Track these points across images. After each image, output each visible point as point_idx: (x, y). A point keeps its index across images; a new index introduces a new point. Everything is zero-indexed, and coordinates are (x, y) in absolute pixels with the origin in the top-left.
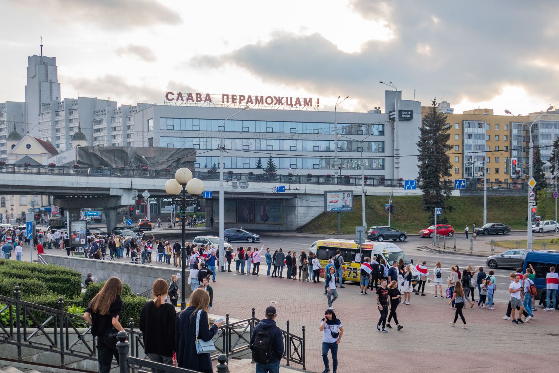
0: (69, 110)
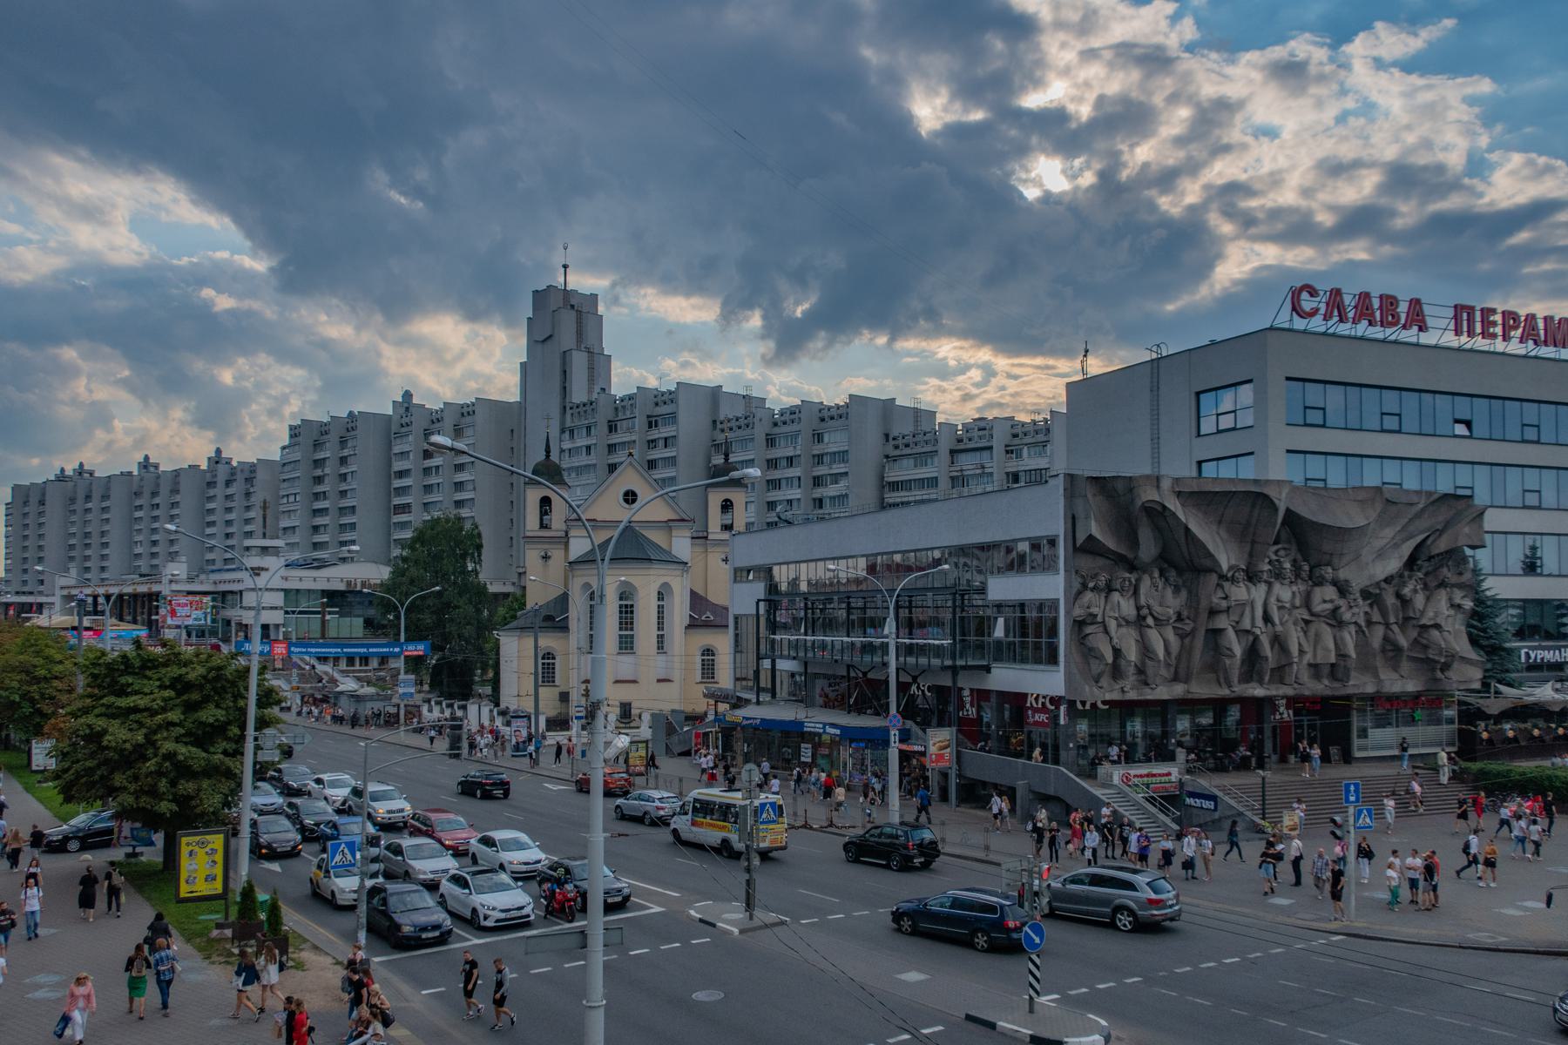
0: (648, 417)
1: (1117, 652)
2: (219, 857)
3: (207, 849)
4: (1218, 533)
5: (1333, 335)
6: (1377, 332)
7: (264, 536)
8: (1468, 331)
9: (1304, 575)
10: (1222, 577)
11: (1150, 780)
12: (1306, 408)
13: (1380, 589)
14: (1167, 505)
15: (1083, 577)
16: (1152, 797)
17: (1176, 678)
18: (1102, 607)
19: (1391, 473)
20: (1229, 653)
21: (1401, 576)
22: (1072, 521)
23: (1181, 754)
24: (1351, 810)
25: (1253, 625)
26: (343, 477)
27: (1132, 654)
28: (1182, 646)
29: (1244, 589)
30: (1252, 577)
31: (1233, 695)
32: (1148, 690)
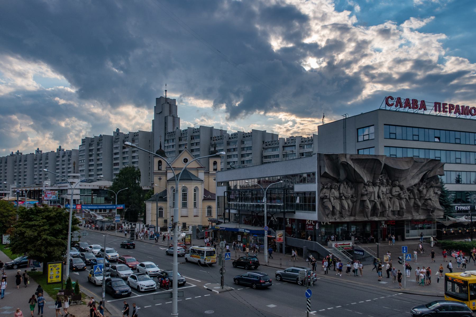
0: (191, 136)
1: (333, 207)
2: (60, 270)
3: (56, 268)
4: (364, 171)
5: (398, 111)
6: (411, 111)
7: (74, 173)
8: (439, 110)
9: (390, 184)
10: (365, 184)
12: (390, 133)
13: (413, 188)
14: (349, 163)
15: (323, 184)
16: (344, 251)
17: (351, 215)
18: (329, 193)
19: (416, 153)
20: (367, 207)
21: (419, 184)
22: (320, 168)
23: (353, 238)
24: (404, 255)
25: (375, 199)
26: (98, 155)
27: (338, 208)
28: (353, 206)
29: (372, 188)
30: (374, 184)
31: (368, 220)
32: (343, 219)
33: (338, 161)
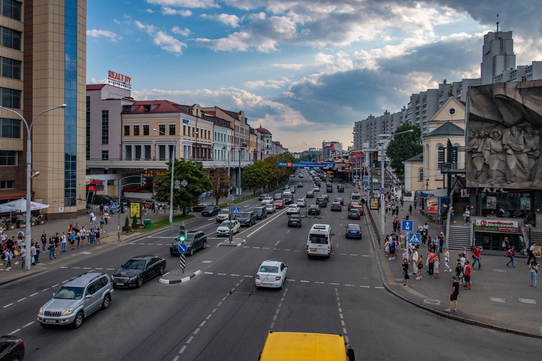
0: (522, 77)
2: (139, 209)
11: (499, 225)
14: (508, 95)
15: (473, 132)
27: (495, 166)
33: (493, 94)
